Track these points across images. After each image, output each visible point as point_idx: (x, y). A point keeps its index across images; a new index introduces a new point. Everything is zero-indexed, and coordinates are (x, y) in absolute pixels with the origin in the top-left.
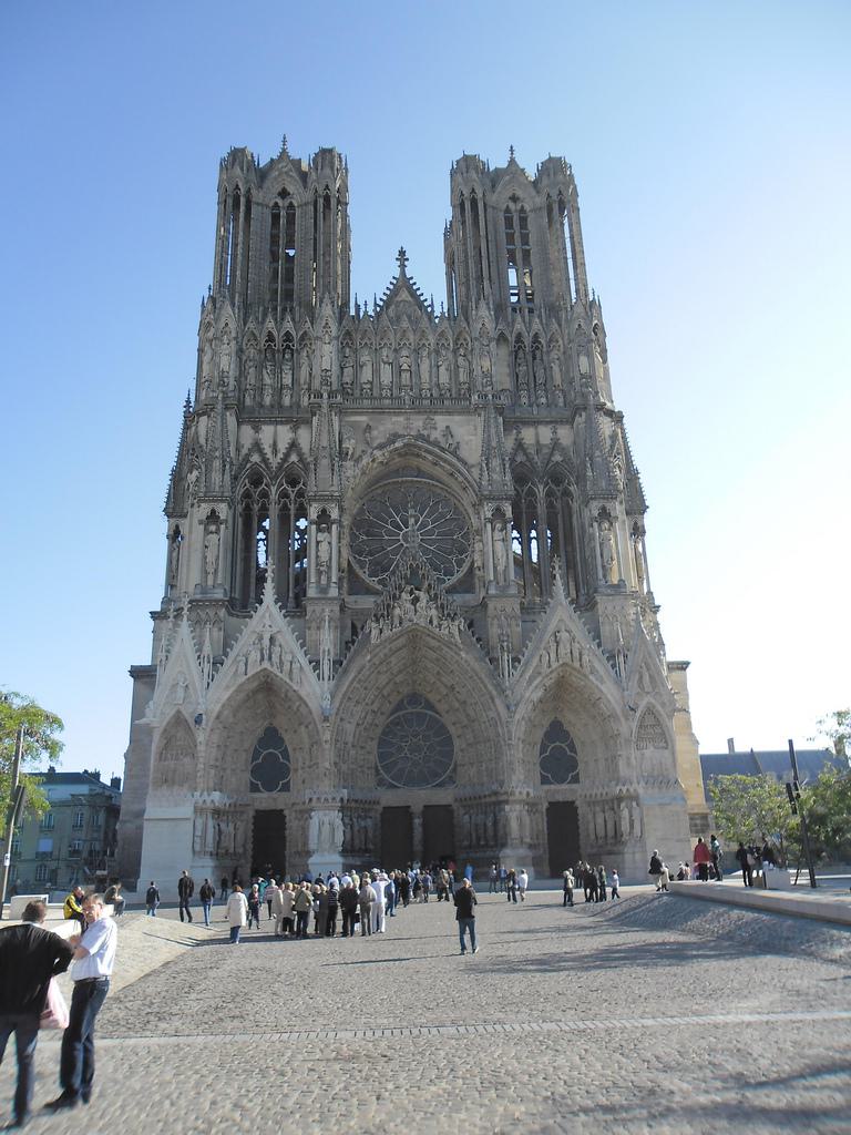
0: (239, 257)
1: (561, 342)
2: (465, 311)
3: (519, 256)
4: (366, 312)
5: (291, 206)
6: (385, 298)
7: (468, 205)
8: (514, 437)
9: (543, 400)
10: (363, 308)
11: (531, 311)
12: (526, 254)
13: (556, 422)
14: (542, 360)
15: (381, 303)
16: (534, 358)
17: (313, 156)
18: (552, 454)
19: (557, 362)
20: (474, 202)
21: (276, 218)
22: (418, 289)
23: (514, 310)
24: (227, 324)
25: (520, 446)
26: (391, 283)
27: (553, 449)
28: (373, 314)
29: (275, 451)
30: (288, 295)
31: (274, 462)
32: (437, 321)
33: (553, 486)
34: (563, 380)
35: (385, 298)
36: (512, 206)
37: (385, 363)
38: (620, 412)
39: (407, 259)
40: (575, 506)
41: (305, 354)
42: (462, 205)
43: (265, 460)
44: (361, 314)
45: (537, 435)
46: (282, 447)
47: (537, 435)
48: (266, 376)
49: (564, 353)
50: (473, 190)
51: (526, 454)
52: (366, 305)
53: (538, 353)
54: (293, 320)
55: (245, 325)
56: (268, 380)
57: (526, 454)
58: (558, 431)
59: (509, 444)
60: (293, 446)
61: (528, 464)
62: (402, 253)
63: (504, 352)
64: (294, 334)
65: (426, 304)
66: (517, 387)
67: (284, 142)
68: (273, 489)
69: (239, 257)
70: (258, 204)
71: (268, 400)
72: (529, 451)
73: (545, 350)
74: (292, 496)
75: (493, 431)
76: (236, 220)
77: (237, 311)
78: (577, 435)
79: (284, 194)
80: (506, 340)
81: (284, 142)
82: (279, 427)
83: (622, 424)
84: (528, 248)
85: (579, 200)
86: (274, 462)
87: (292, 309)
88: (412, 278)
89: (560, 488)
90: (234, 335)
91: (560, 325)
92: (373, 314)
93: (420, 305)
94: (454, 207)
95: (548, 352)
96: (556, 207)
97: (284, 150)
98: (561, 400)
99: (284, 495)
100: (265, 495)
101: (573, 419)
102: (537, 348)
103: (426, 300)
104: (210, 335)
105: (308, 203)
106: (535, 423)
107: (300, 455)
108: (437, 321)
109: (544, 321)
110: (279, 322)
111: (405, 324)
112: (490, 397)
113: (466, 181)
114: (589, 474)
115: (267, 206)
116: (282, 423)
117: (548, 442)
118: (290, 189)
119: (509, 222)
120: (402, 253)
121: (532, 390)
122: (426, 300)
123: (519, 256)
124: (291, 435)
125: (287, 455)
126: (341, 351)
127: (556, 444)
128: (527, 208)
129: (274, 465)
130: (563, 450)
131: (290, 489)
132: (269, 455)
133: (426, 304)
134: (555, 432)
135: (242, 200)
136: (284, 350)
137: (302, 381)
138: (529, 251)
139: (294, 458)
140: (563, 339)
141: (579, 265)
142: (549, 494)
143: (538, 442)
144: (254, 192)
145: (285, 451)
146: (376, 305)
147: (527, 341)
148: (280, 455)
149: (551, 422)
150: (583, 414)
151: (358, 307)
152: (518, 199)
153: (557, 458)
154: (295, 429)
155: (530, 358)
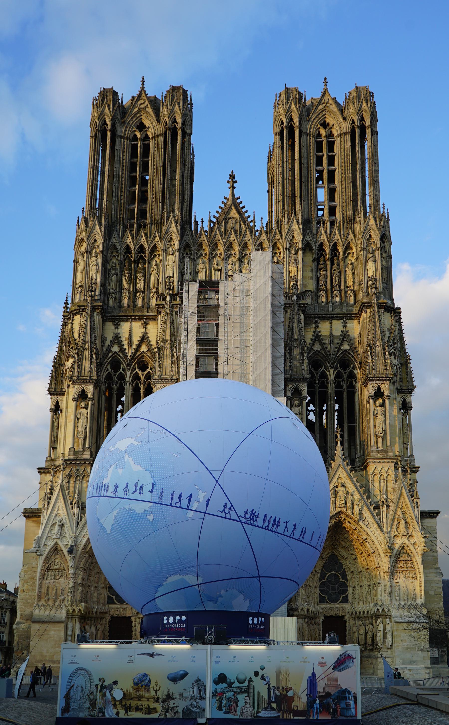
0: (106, 183)
1: (354, 250)
2: (279, 223)
3: (325, 176)
4: (202, 228)
5: (147, 137)
6: (217, 215)
7: (286, 132)
8: (313, 330)
9: (338, 299)
10: (200, 223)
11: (332, 223)
12: (331, 174)
13: (347, 318)
14: (339, 265)
15: (214, 220)
16: (332, 264)
17: (165, 93)
18: (341, 344)
19: (351, 267)
20: (291, 130)
21: (134, 147)
22: (244, 207)
23: (319, 223)
24: (95, 240)
25: (317, 337)
26: (220, 207)
27: (343, 340)
28: (208, 229)
29: (131, 342)
30: (143, 213)
31: (129, 351)
32: (257, 234)
33: (342, 371)
34: (354, 282)
35: (217, 215)
36: (323, 132)
37: (215, 270)
38: (399, 308)
39: (236, 182)
40: (358, 386)
41: (154, 263)
42: (281, 133)
43: (123, 350)
44: (199, 229)
45: (331, 328)
46: (136, 339)
47: (331, 328)
48: (125, 282)
49: (357, 259)
50: (291, 118)
51: (321, 344)
52: (202, 222)
53: (336, 262)
54: (146, 234)
55: (109, 239)
56: (126, 285)
57: (321, 344)
58: (348, 325)
59: (309, 336)
60: (144, 338)
61: (322, 352)
62: (232, 176)
63: (310, 258)
64: (146, 246)
65: (249, 219)
66: (318, 289)
67: (143, 81)
68: (128, 373)
69: (106, 183)
70: (121, 137)
71: (125, 301)
72: (324, 342)
73: (342, 256)
74: (142, 379)
75: (296, 325)
76: (104, 151)
77: (103, 229)
78: (362, 328)
79: (141, 127)
80: (311, 249)
81: (143, 81)
82: (134, 323)
83: (400, 318)
84: (332, 168)
85: (378, 124)
86: (129, 351)
87: (145, 225)
88: (239, 198)
89: (348, 371)
90: (100, 248)
91: (355, 236)
92: (208, 229)
93: (244, 219)
94: (276, 134)
95: (345, 258)
96: (357, 131)
97: (143, 89)
98: (352, 298)
99: (136, 377)
100: (122, 377)
101: (360, 315)
102: (336, 255)
103: (249, 216)
104: (83, 249)
105: (158, 136)
106: (330, 317)
107: (149, 345)
108: (257, 234)
109: (342, 233)
110: (136, 237)
111: (233, 237)
112: (295, 297)
113: (288, 111)
114: (370, 361)
115: (128, 139)
116: (136, 320)
117: (339, 333)
118: (147, 123)
119: (319, 147)
120: (232, 176)
121: (329, 292)
122: (249, 216)
123: (325, 176)
124: (143, 330)
125: (139, 346)
126: (181, 260)
127: (345, 336)
128: (335, 133)
129: (129, 354)
130: (351, 341)
131: (140, 373)
132: (126, 347)
133: (249, 219)
134: (345, 326)
135: (109, 134)
136: (139, 260)
137: (152, 286)
138: (334, 171)
139: (144, 348)
140: (356, 247)
141: (375, 183)
142: (338, 376)
143: (331, 334)
144: (118, 126)
145: (137, 343)
146: (211, 221)
147: (327, 249)
148: (134, 346)
149: (342, 318)
150: (368, 311)
151: (196, 223)
152: (328, 125)
153: (346, 347)
154: (145, 325)
155: (328, 263)
